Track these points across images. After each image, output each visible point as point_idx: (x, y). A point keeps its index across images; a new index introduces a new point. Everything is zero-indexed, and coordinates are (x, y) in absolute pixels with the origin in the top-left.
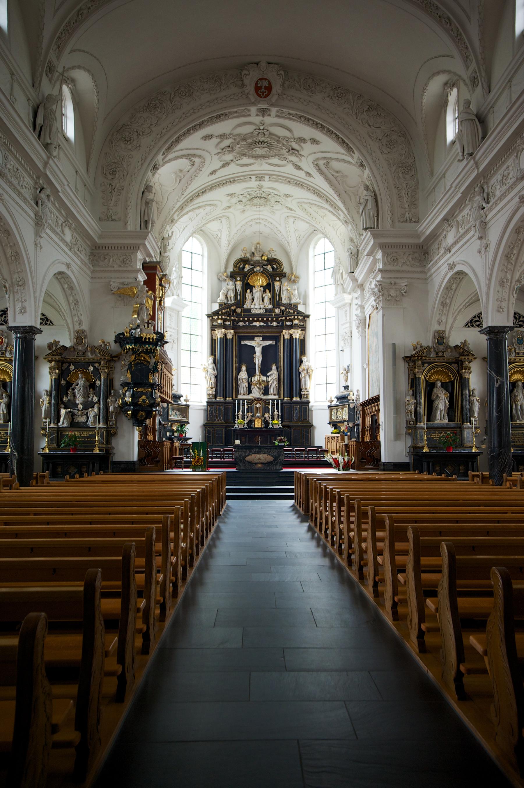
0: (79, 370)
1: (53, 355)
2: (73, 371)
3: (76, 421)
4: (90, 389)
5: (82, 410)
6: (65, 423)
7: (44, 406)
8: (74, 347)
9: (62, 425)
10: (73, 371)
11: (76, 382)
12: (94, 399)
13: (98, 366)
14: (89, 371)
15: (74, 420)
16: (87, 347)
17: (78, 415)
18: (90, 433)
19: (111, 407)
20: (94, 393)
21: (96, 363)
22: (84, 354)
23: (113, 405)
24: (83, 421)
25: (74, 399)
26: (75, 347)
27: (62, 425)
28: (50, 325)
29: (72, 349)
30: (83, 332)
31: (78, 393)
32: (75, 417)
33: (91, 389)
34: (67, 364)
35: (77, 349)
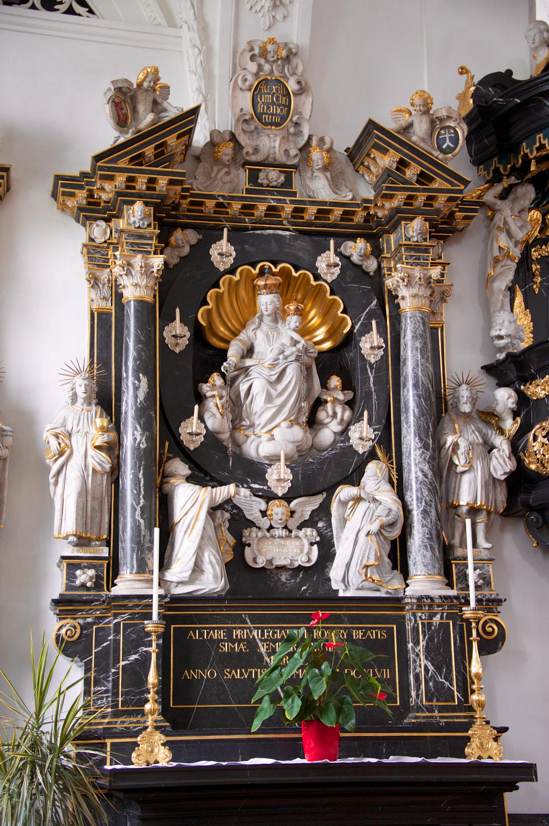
0: (262, 269)
1: (138, 159)
2: (232, 271)
3: (261, 563)
4: (324, 385)
5: (288, 498)
6: (207, 567)
7: (76, 462)
8: (233, 137)
9: (191, 580)
10: (232, 271)
11: (242, 336)
12: (354, 433)
13: (364, 257)
14: (317, 277)
15: (248, 553)
16: (308, 144)
17: (265, 523)
18: (358, 635)
19: (466, 480)
20: (350, 404)
21: (353, 237)
22: (288, 182)
23: (478, 466)
24: (301, 560)
25: (232, 436)
26: (243, 139)
27: (191, 580)
28: (70, 11)
29: (226, 151)
30: (287, 59)
31: (269, 398)
32: (253, 534)
33: (335, 381)
34: (192, 236)
35: (256, 150)
